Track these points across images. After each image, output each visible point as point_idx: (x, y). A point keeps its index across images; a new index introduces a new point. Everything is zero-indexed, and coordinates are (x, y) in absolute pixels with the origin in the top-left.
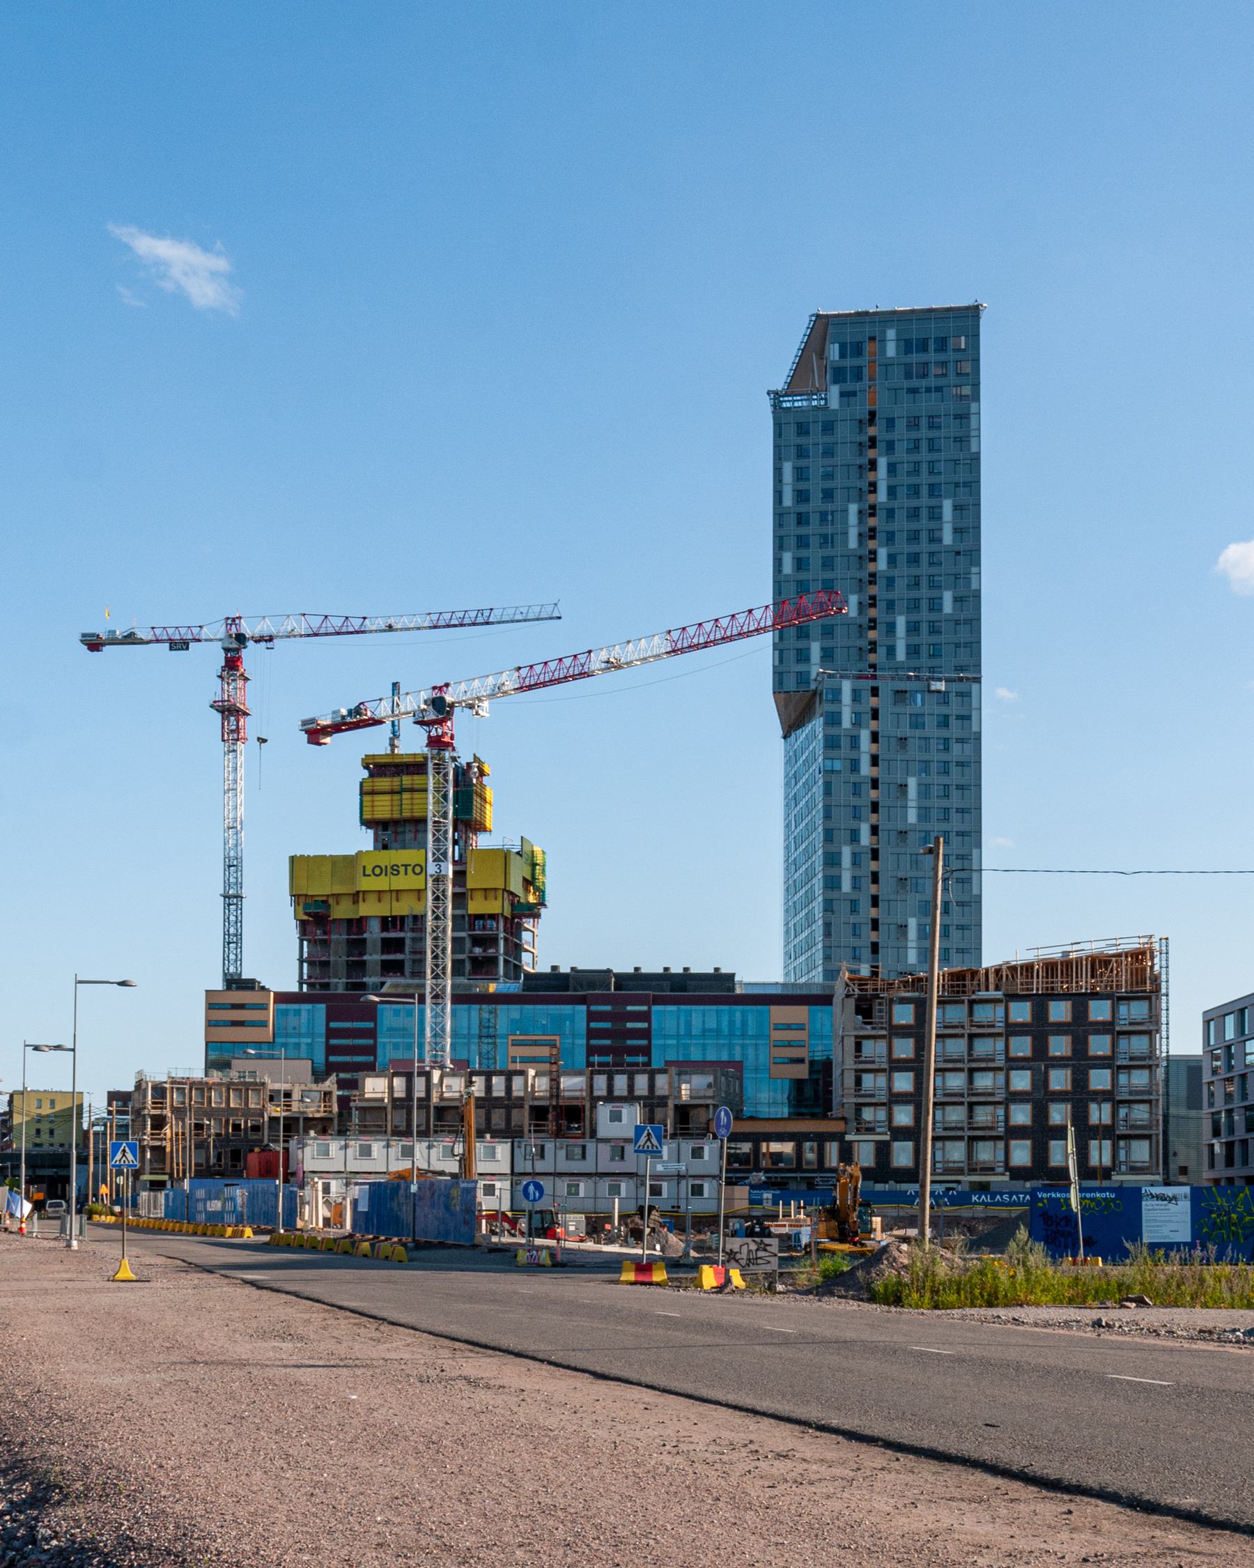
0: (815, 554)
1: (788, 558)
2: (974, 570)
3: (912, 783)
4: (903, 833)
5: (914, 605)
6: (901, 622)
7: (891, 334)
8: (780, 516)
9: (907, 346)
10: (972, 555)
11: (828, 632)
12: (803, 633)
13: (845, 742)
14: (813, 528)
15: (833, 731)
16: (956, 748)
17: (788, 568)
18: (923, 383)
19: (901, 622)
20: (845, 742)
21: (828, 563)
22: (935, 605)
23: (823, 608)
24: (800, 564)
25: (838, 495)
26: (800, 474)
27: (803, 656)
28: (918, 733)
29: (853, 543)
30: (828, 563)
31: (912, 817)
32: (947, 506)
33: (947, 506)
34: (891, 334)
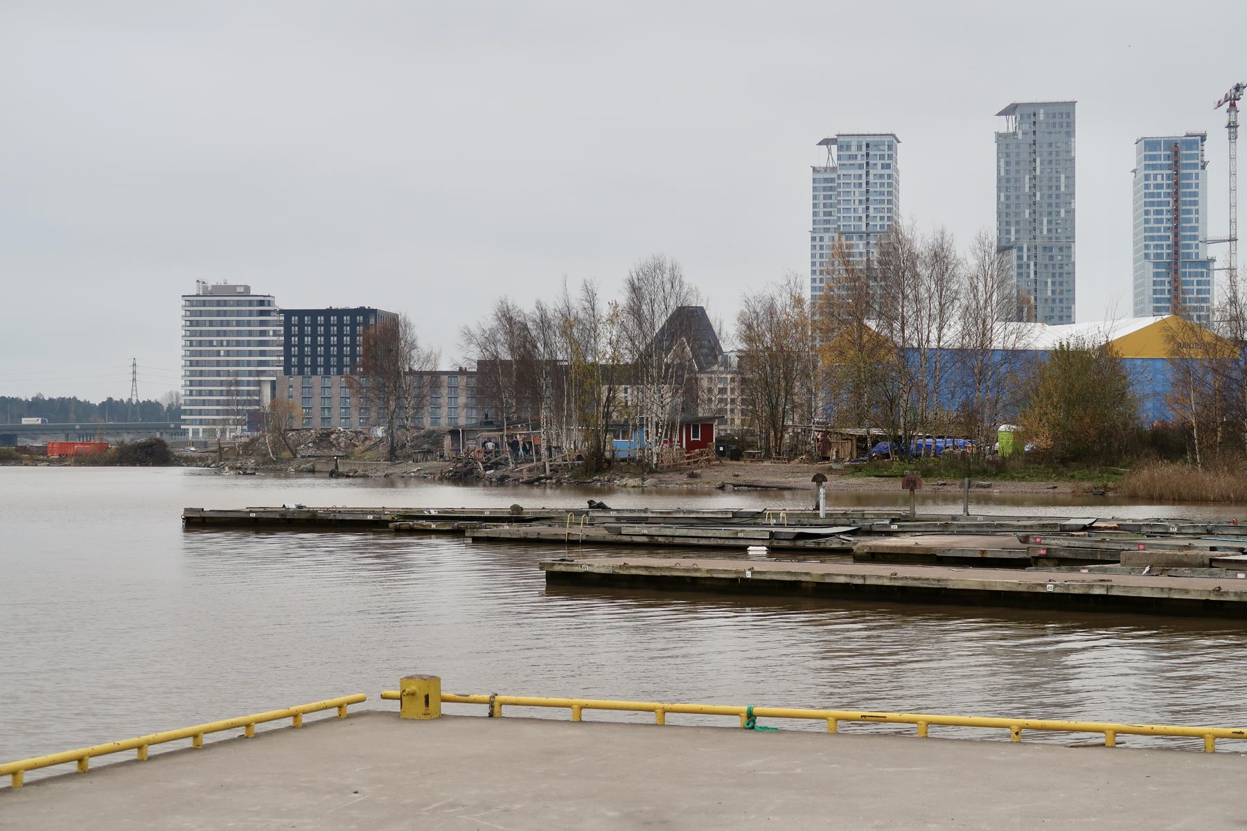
0: (1013, 194)
1: (1002, 195)
2: (1072, 201)
3: (1049, 281)
4: (1046, 300)
5: (1050, 213)
6: (1045, 220)
7: (1042, 111)
8: (999, 180)
9: (1047, 115)
10: (1072, 195)
11: (1017, 223)
12: (1008, 223)
13: (1025, 266)
14: (1012, 184)
15: (1020, 262)
16: (1065, 267)
17: (1002, 199)
18: (1054, 130)
19: (1045, 220)
20: (1025, 266)
21: (1017, 197)
22: (1058, 213)
23: (1016, 214)
24: (1008, 198)
25: (1021, 172)
26: (1007, 163)
27: (1008, 232)
28: (1051, 262)
29: (1027, 190)
30: (1017, 197)
31: (1049, 293)
32: (1063, 177)
33: (1063, 177)
34: (1042, 111)
